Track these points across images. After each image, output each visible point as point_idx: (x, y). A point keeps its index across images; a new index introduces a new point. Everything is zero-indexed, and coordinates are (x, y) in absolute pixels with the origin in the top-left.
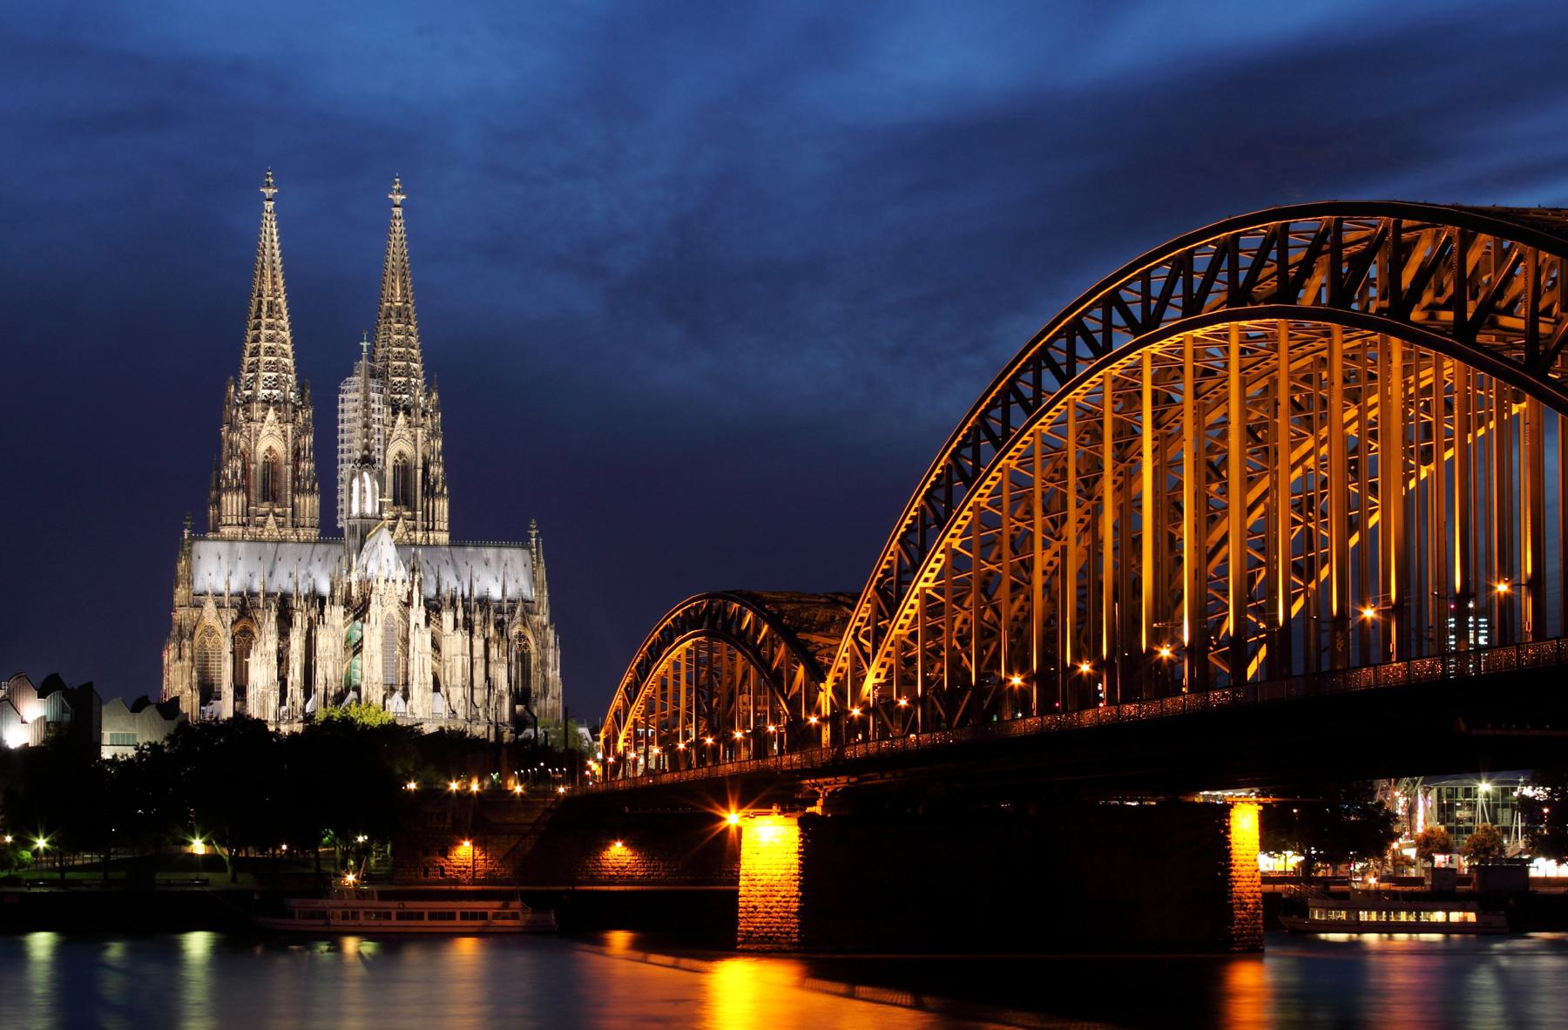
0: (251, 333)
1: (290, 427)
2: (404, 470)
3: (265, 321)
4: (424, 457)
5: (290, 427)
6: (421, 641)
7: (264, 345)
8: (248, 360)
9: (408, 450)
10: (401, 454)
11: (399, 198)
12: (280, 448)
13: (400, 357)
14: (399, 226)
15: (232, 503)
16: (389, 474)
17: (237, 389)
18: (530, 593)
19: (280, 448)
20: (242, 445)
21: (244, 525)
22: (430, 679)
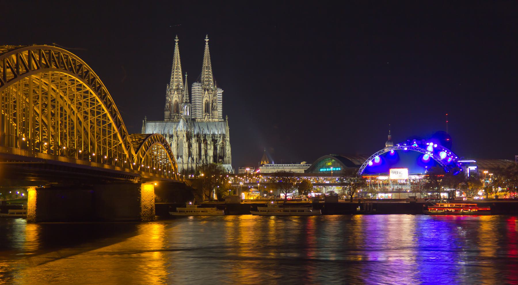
0: (172, 74)
1: (180, 95)
2: (207, 105)
3: (175, 70)
4: (212, 101)
5: (180, 95)
6: (186, 145)
7: (175, 76)
8: (172, 80)
9: (208, 100)
10: (207, 100)
11: (207, 40)
12: (178, 100)
13: (207, 78)
14: (207, 47)
15: (167, 113)
16: (204, 105)
17: (169, 87)
18: (224, 132)
19: (178, 100)
20: (170, 100)
21: (170, 119)
22: (187, 154)
